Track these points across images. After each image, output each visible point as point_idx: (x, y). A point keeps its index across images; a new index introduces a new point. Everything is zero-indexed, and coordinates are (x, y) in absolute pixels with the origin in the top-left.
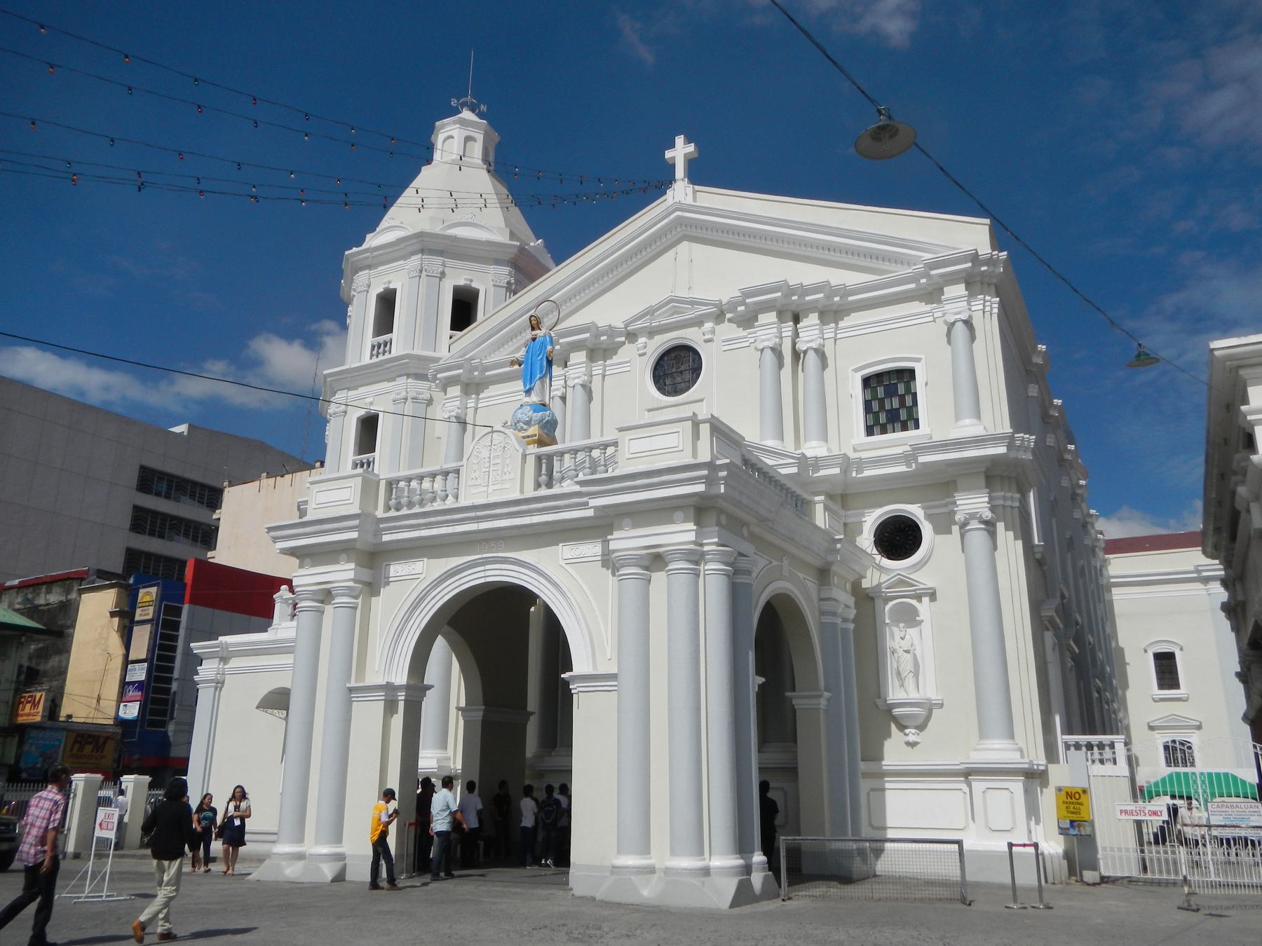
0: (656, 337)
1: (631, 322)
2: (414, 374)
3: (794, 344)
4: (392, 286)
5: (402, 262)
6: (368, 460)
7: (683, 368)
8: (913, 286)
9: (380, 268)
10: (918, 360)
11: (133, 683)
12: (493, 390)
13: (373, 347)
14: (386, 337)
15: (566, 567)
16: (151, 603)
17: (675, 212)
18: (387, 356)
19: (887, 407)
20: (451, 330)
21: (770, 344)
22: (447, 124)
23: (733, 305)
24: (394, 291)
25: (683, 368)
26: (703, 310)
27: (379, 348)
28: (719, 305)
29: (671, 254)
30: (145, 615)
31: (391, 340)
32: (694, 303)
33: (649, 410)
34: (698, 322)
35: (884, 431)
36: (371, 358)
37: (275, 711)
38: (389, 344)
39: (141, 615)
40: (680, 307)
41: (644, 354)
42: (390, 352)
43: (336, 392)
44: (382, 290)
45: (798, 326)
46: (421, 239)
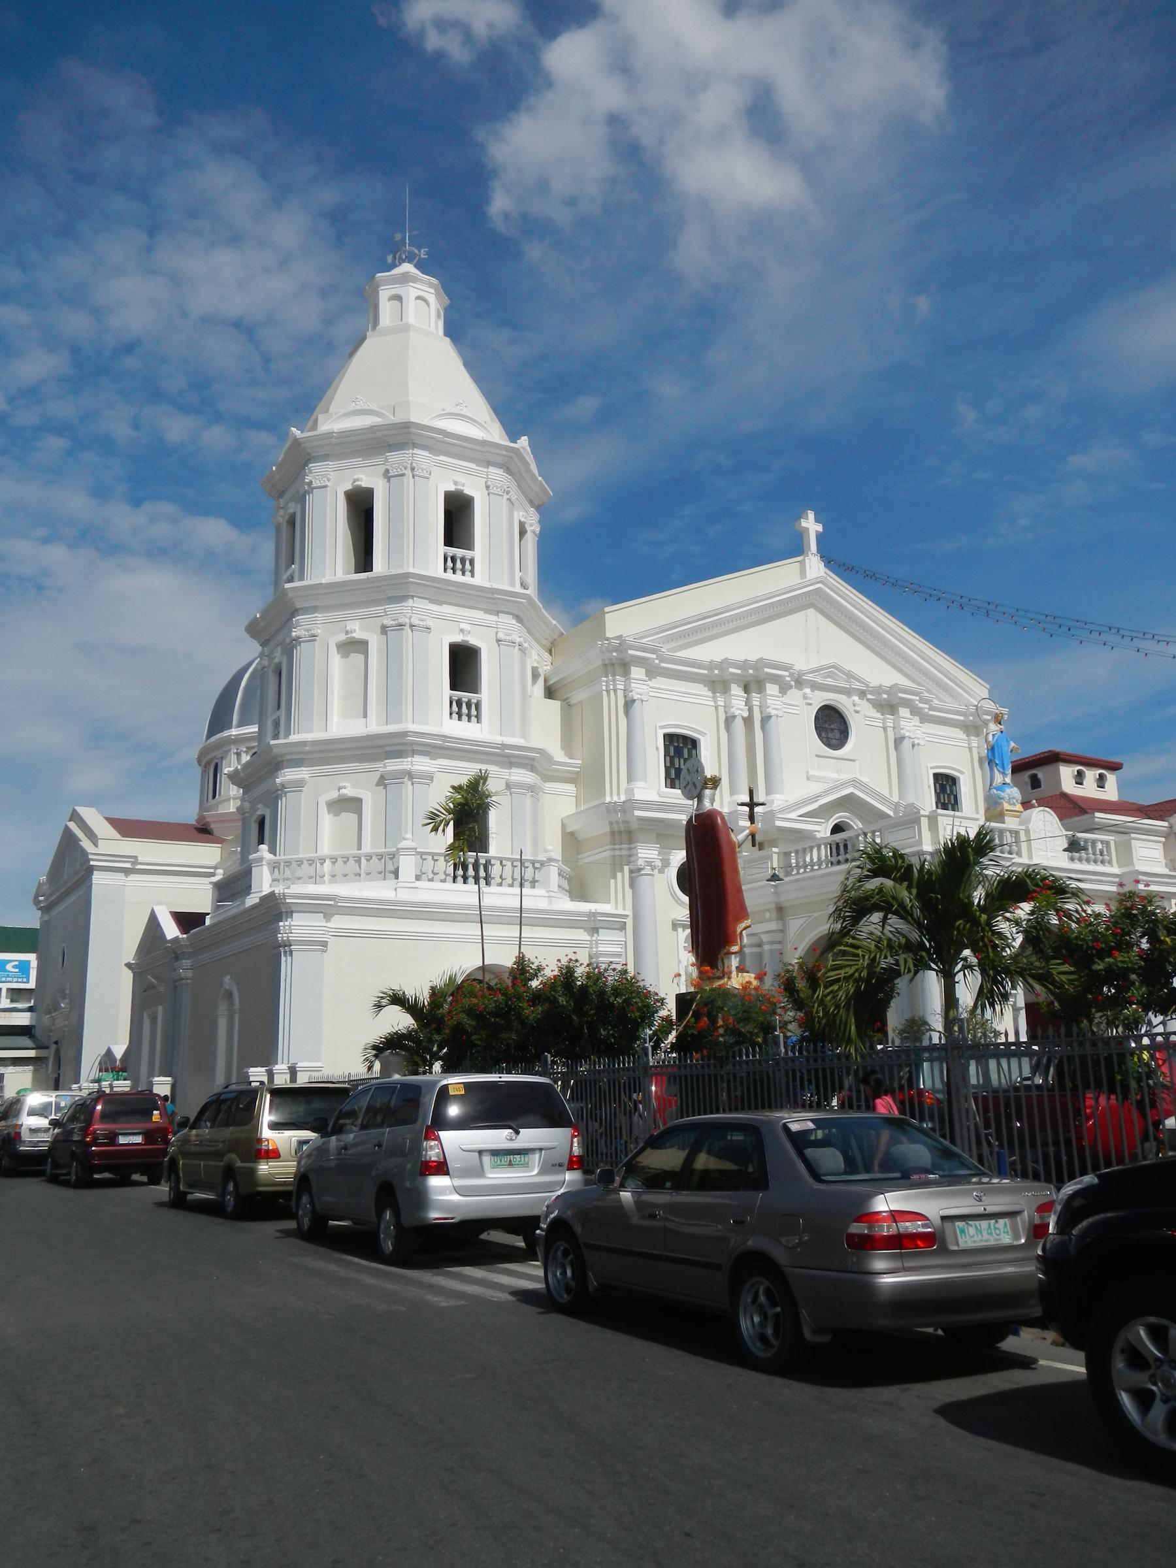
0: (817, 692)
1: (807, 673)
2: (517, 616)
5: (473, 466)
7: (832, 726)
8: (962, 718)
9: (442, 458)
10: (962, 773)
12: (660, 682)
17: (818, 583)
18: (467, 579)
19: (942, 801)
22: (422, 281)
23: (878, 690)
25: (832, 726)
26: (856, 685)
28: (867, 686)
29: (802, 614)
32: (850, 676)
33: (817, 756)
34: (848, 692)
36: (445, 570)
40: (839, 676)
41: (810, 704)
42: (473, 576)
43: (413, 597)
44: (453, 490)
46: (512, 455)
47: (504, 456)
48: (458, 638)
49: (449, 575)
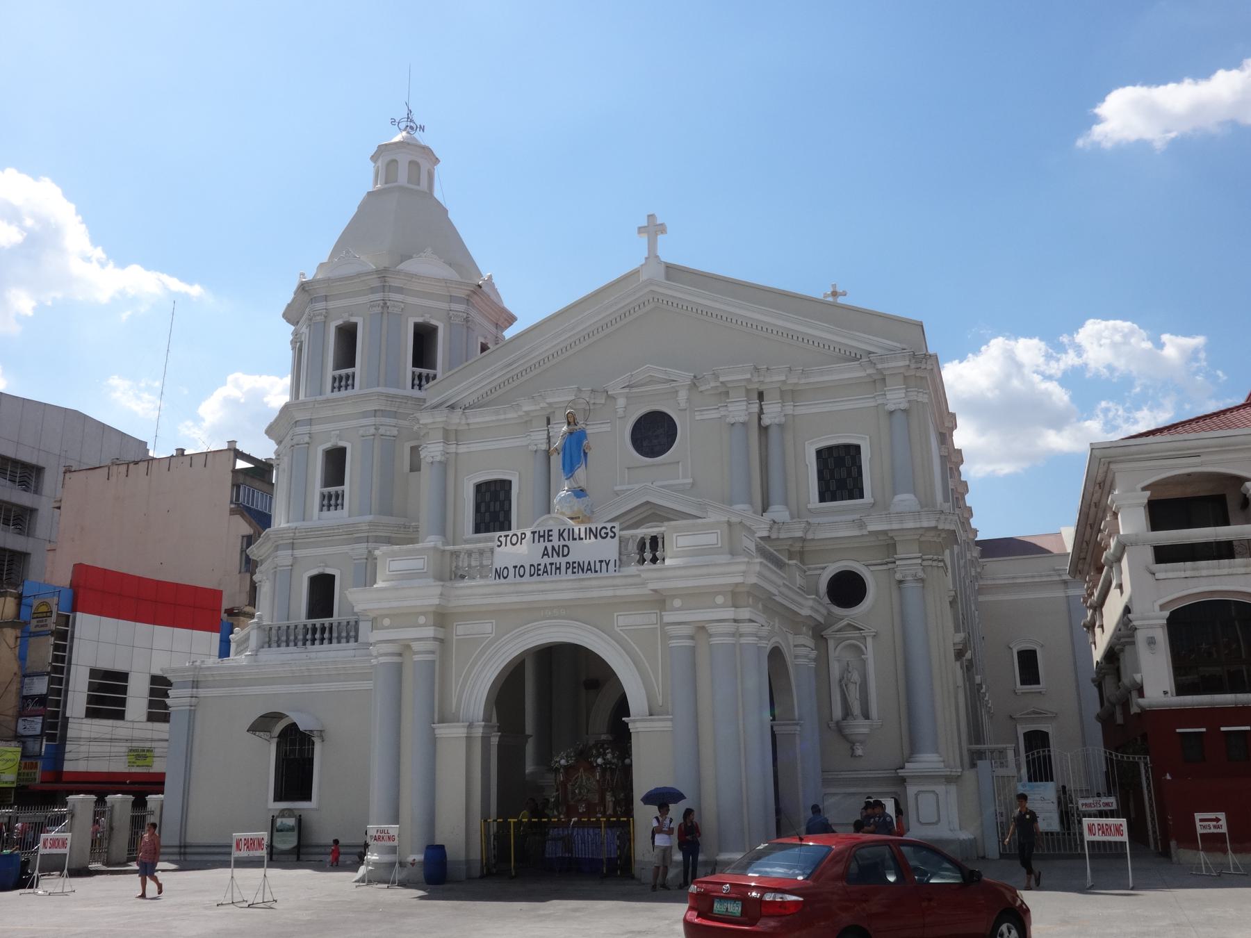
3: (760, 419)
4: (353, 320)
6: (336, 492)
11: (32, 697)
13: (334, 379)
14: (349, 371)
15: (621, 633)
16: (48, 614)
20: (413, 367)
21: (741, 420)
24: (354, 326)
27: (340, 381)
30: (42, 626)
31: (354, 374)
35: (834, 499)
36: (332, 391)
37: (262, 733)
38: (351, 378)
39: (37, 626)
42: (353, 386)
45: (762, 403)
47: (379, 278)
48: (328, 445)
49: (337, 394)
